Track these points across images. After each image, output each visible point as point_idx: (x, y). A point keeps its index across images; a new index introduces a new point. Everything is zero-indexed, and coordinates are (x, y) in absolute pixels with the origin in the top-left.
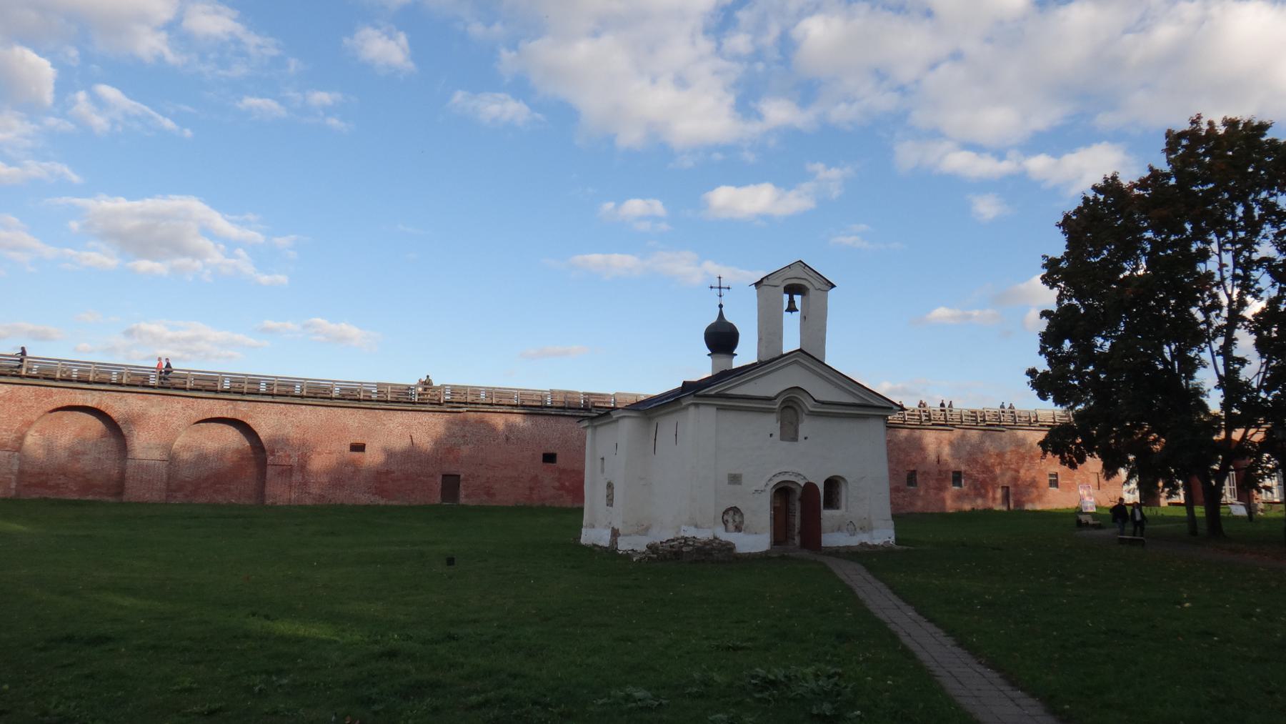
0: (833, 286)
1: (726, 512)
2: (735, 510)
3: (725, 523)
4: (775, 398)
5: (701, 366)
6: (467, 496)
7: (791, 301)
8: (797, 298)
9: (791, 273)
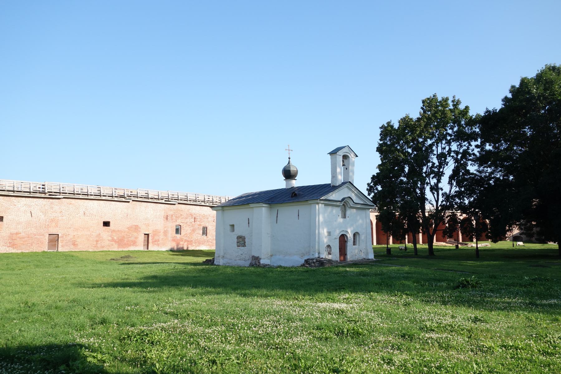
5: (280, 183)
6: (62, 246)
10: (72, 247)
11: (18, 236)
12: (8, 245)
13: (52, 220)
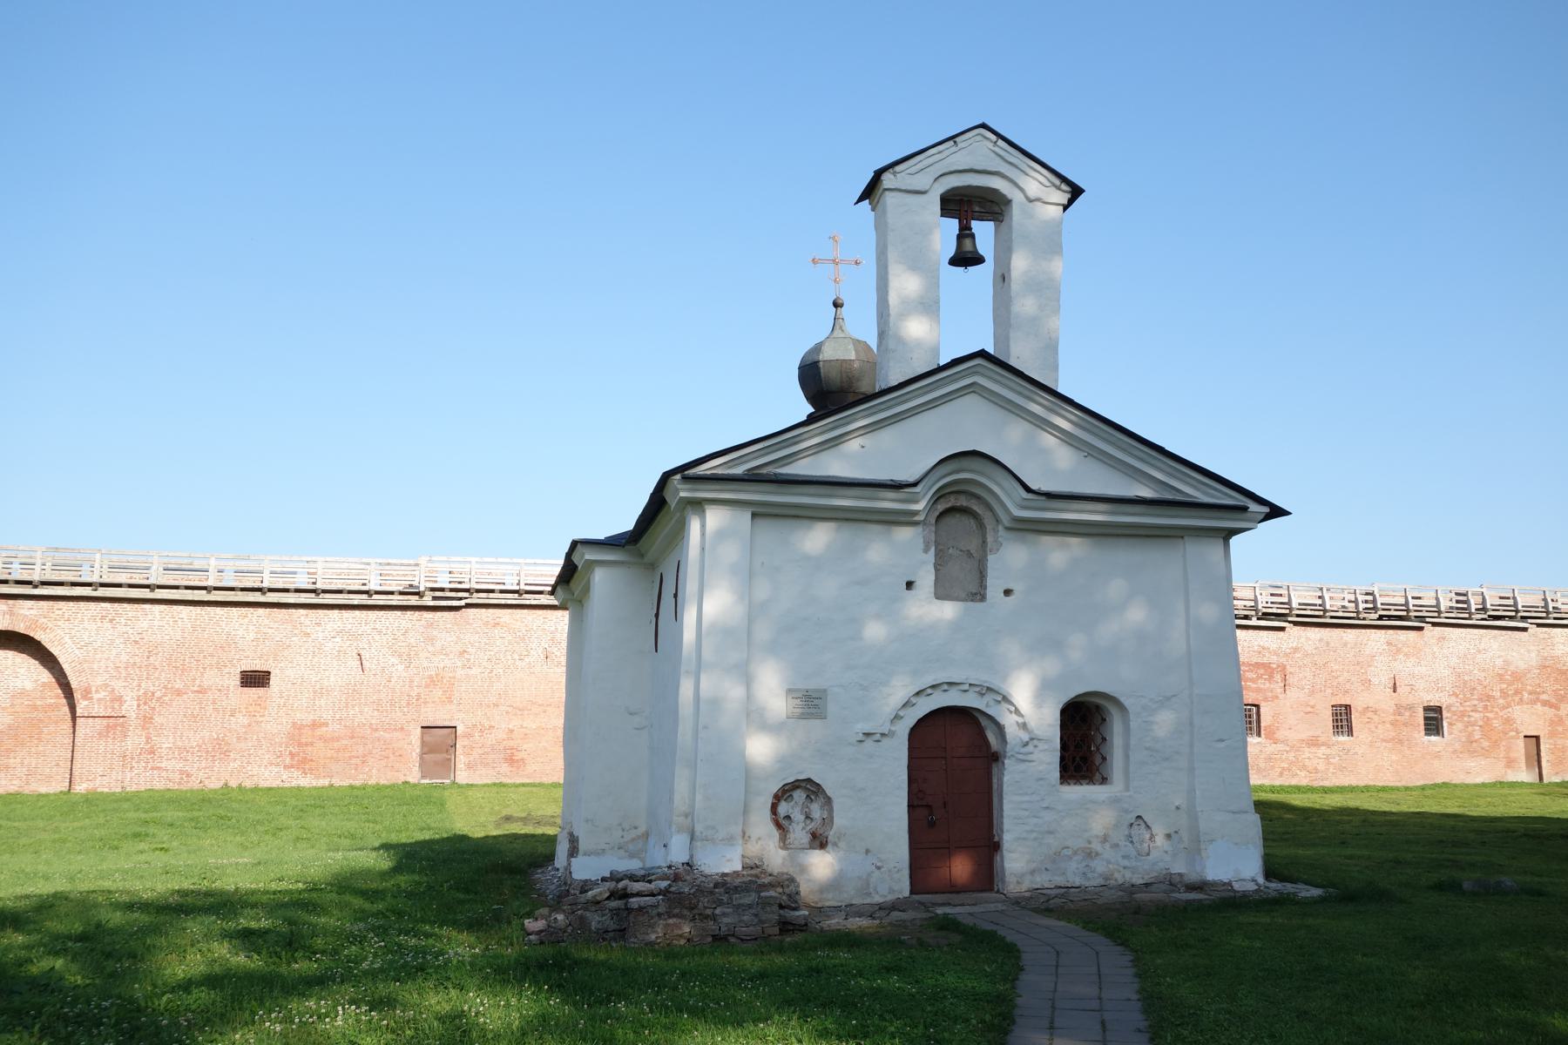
0: (1076, 192)
1: (784, 793)
2: (811, 788)
3: (781, 824)
4: (915, 484)
6: (469, 766)
7: (965, 233)
8: (983, 231)
9: (959, 157)
10: (505, 768)
11: (318, 732)
12: (288, 761)
13: (432, 682)
